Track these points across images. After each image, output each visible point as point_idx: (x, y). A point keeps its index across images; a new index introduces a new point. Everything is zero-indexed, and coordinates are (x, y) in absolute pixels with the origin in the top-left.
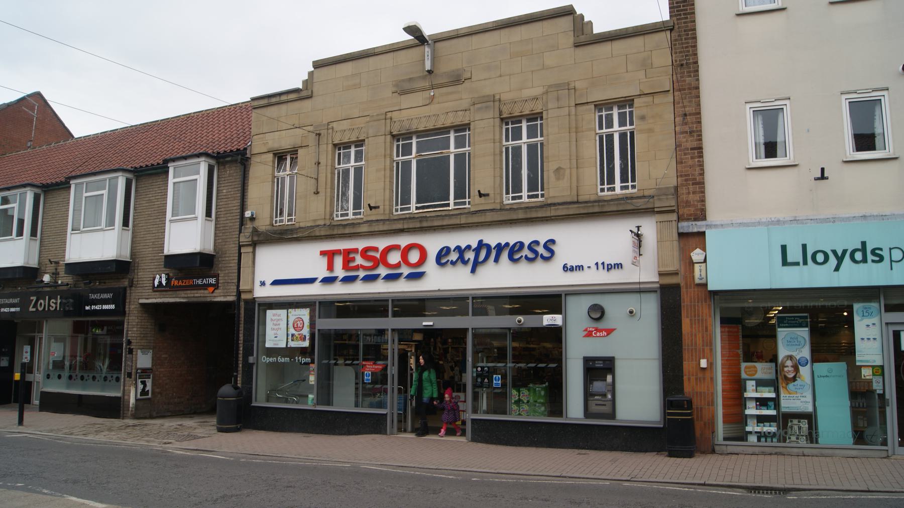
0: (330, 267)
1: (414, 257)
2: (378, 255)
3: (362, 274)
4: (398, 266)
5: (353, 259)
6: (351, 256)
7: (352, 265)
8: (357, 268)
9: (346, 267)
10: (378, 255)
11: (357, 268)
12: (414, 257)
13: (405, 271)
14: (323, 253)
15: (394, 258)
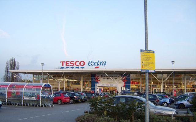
0: (63, 65)
1: (82, 64)
2: (74, 63)
3: (70, 67)
4: (79, 65)
5: (68, 64)
6: (68, 63)
7: (68, 65)
8: (69, 65)
9: (66, 65)
10: (74, 63)
11: (69, 65)
12: (82, 64)
13: (80, 66)
14: (61, 62)
15: (78, 63)
